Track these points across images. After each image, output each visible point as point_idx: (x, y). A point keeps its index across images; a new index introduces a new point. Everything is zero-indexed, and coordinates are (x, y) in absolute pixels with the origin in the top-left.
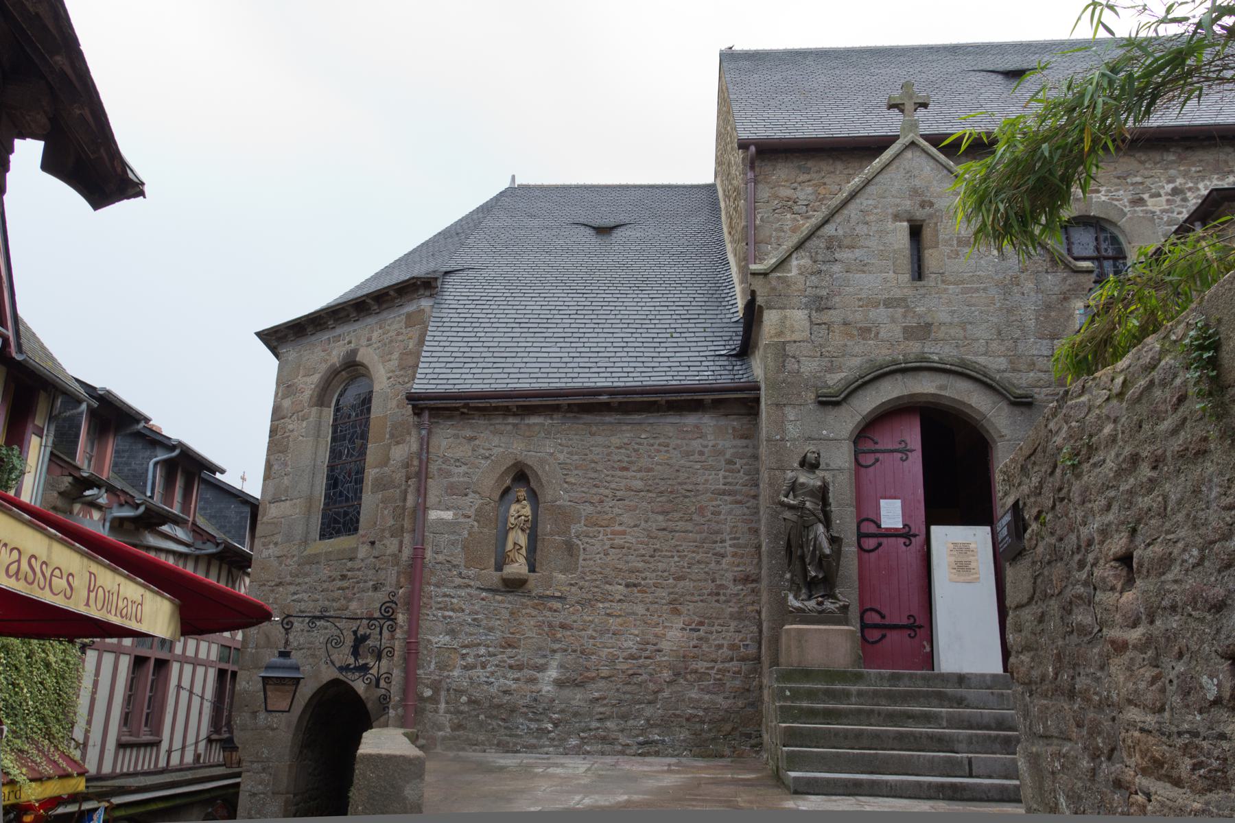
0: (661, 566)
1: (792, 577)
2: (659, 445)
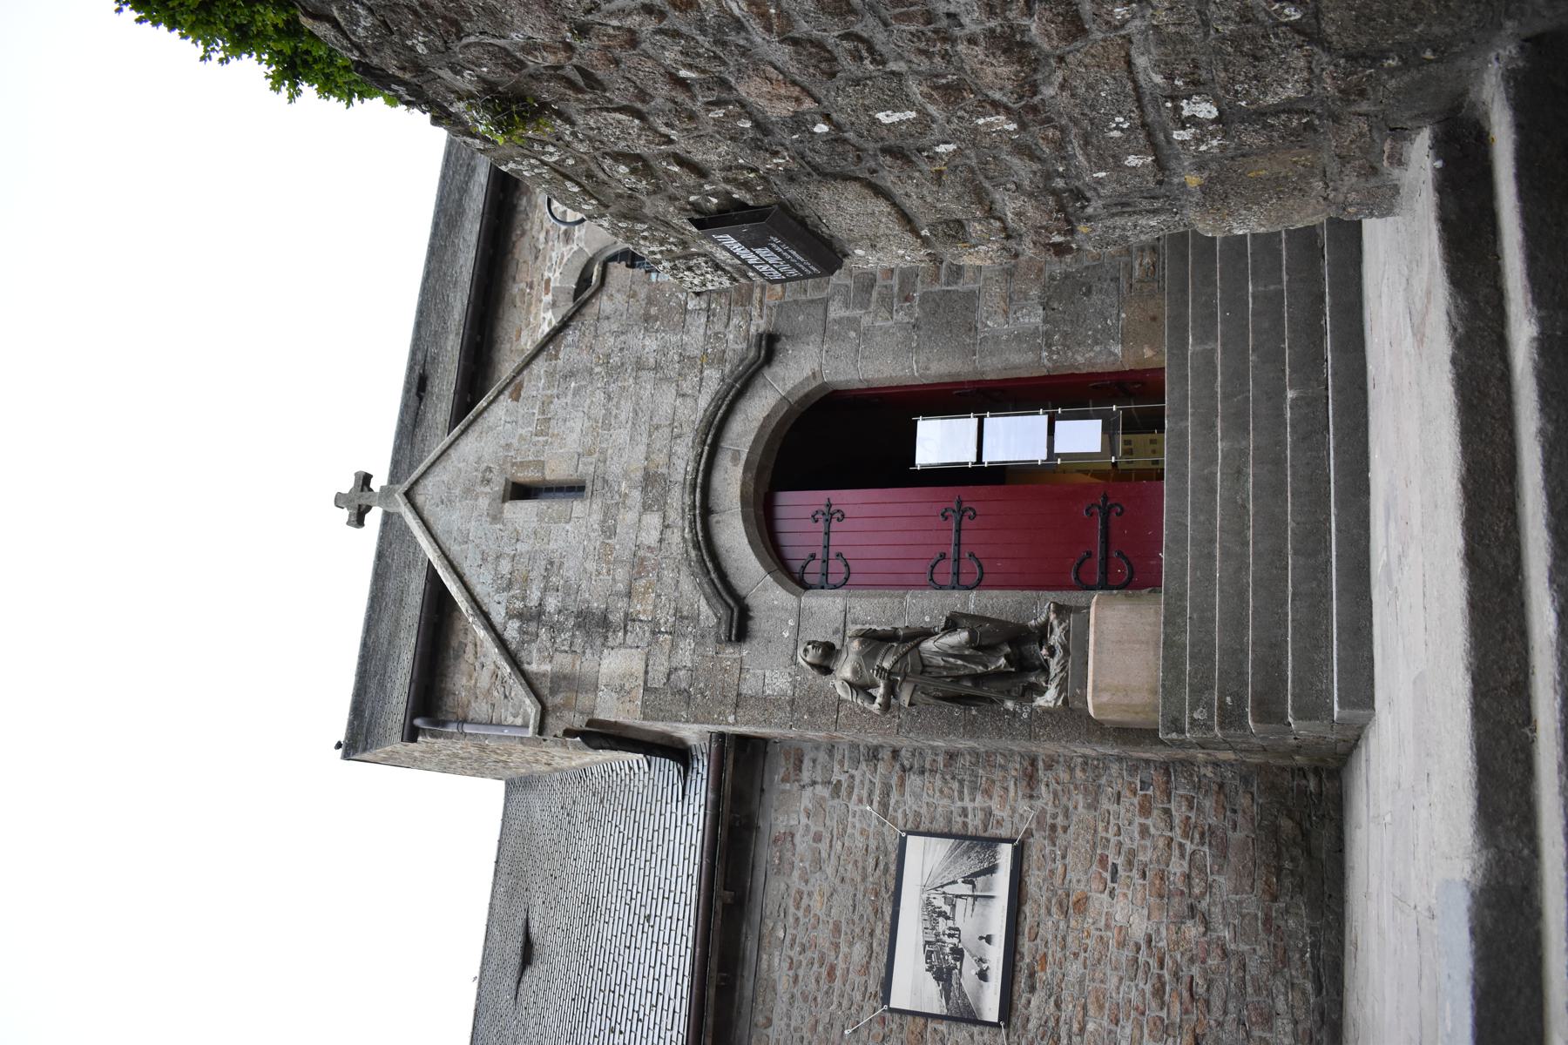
1: (1009, 696)
2: (798, 908)
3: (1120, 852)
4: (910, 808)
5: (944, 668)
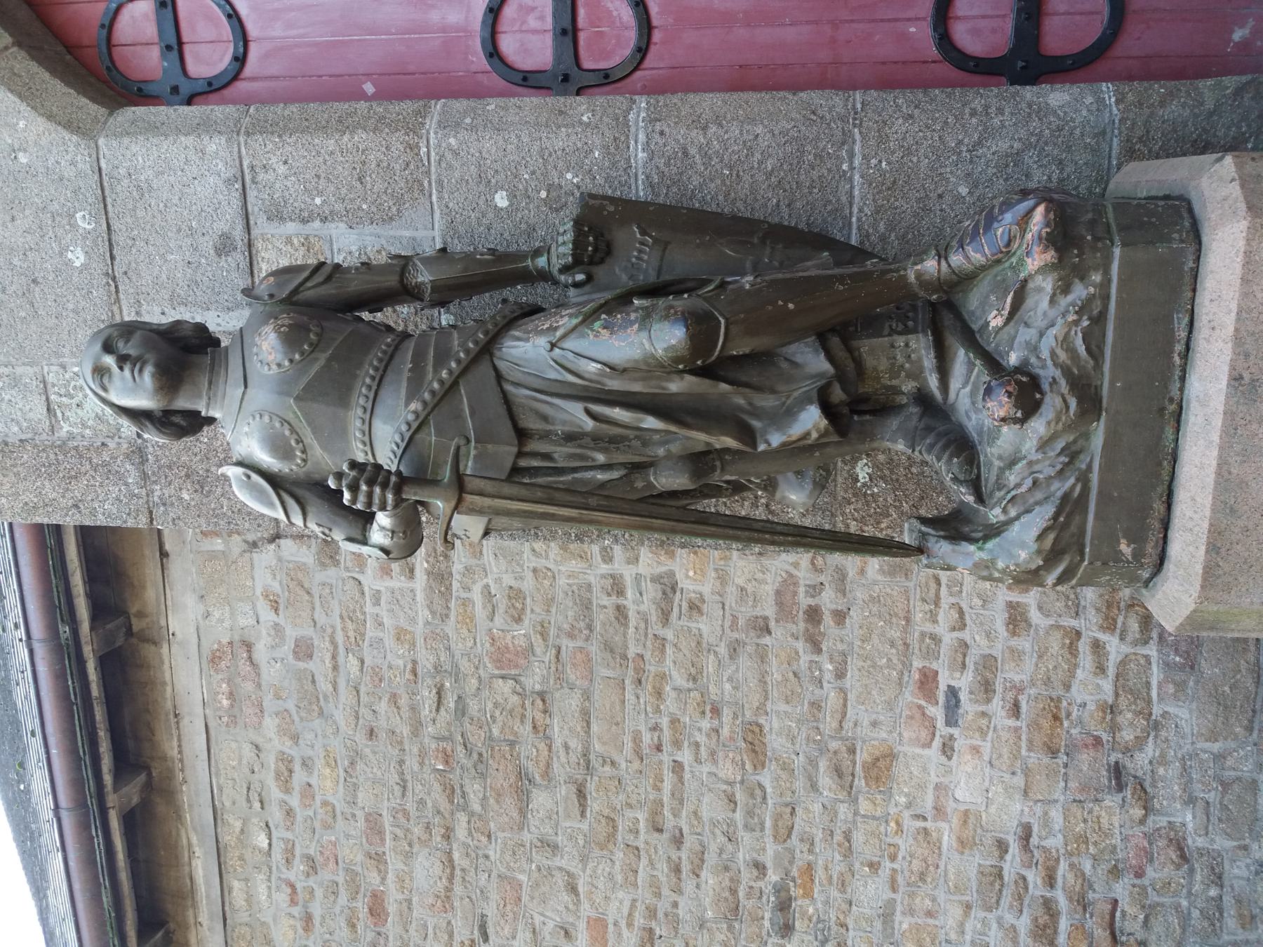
0: (712, 808)
3: (964, 665)
4: (498, 580)
5: (597, 440)
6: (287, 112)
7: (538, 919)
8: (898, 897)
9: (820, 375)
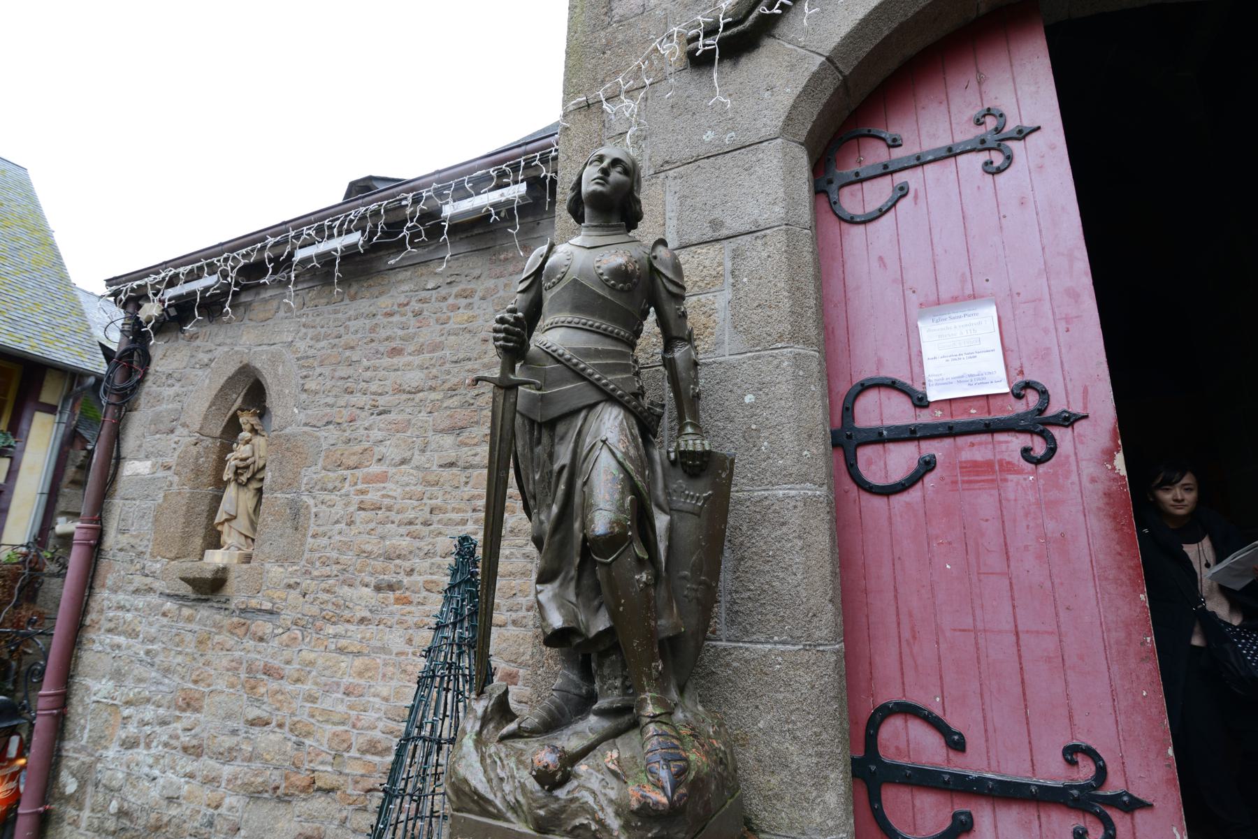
6: (805, 254)
7: (388, 443)
8: (393, 657)
9: (587, 629)
